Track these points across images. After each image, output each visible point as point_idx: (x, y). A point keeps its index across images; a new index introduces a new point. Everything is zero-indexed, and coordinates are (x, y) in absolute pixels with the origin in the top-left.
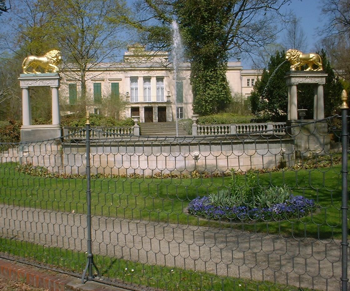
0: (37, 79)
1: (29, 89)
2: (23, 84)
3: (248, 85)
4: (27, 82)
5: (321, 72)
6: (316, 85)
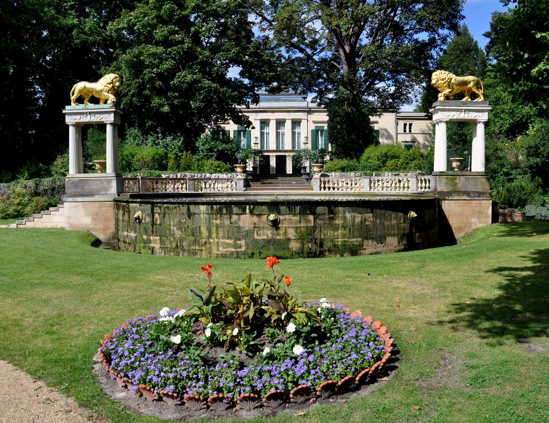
0: (87, 113)
1: (77, 125)
2: (69, 120)
3: (405, 131)
4: (74, 117)
5: (481, 103)
6: (474, 123)
